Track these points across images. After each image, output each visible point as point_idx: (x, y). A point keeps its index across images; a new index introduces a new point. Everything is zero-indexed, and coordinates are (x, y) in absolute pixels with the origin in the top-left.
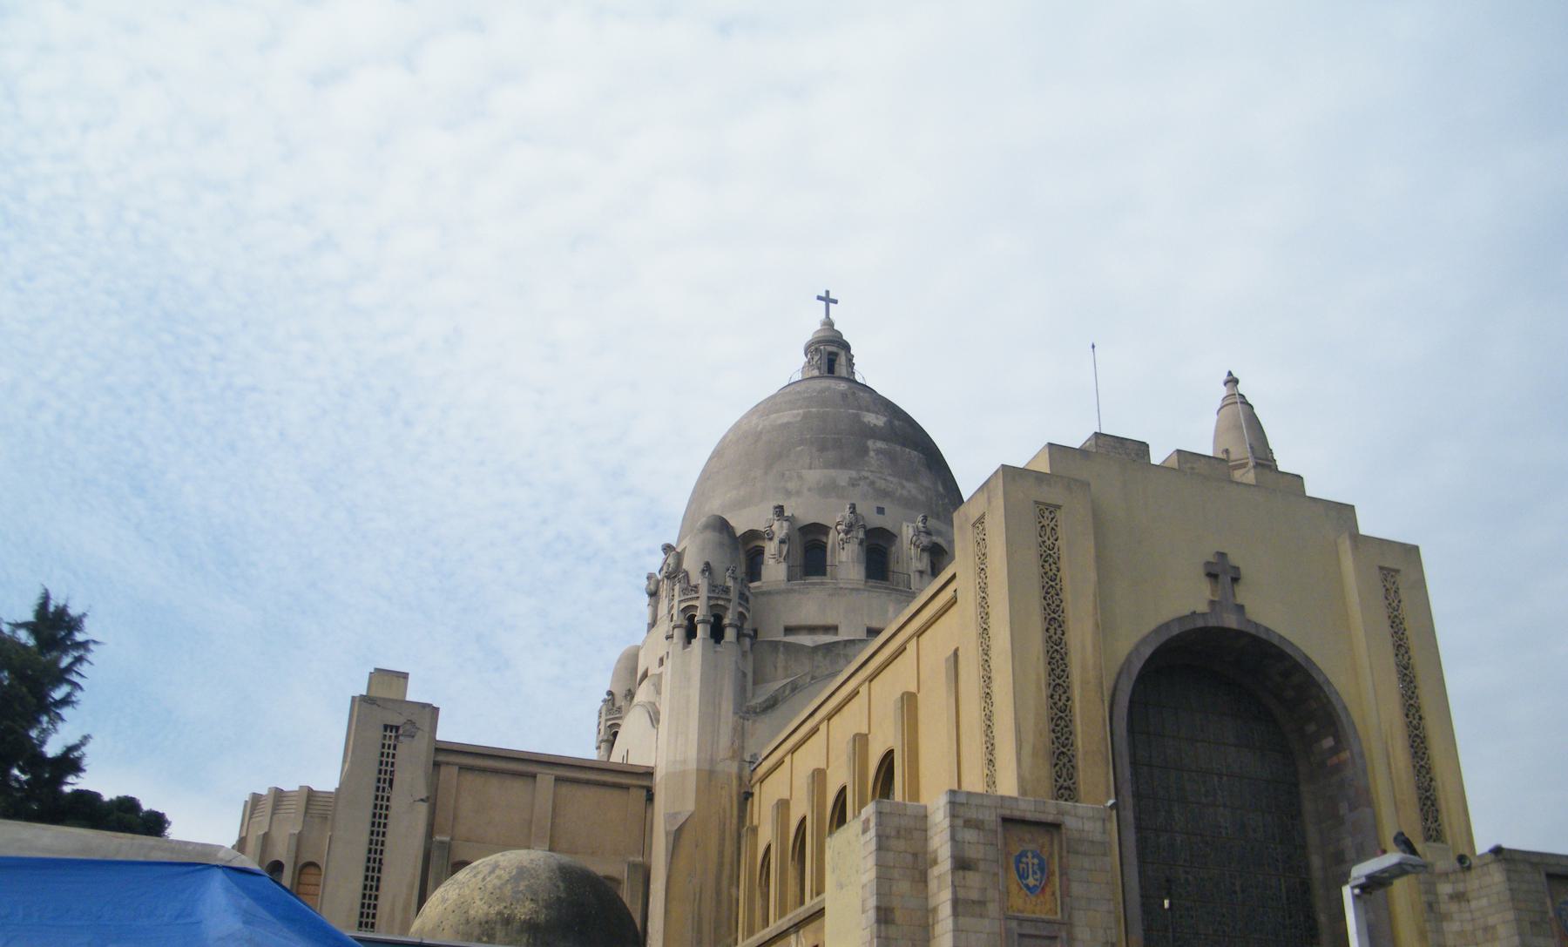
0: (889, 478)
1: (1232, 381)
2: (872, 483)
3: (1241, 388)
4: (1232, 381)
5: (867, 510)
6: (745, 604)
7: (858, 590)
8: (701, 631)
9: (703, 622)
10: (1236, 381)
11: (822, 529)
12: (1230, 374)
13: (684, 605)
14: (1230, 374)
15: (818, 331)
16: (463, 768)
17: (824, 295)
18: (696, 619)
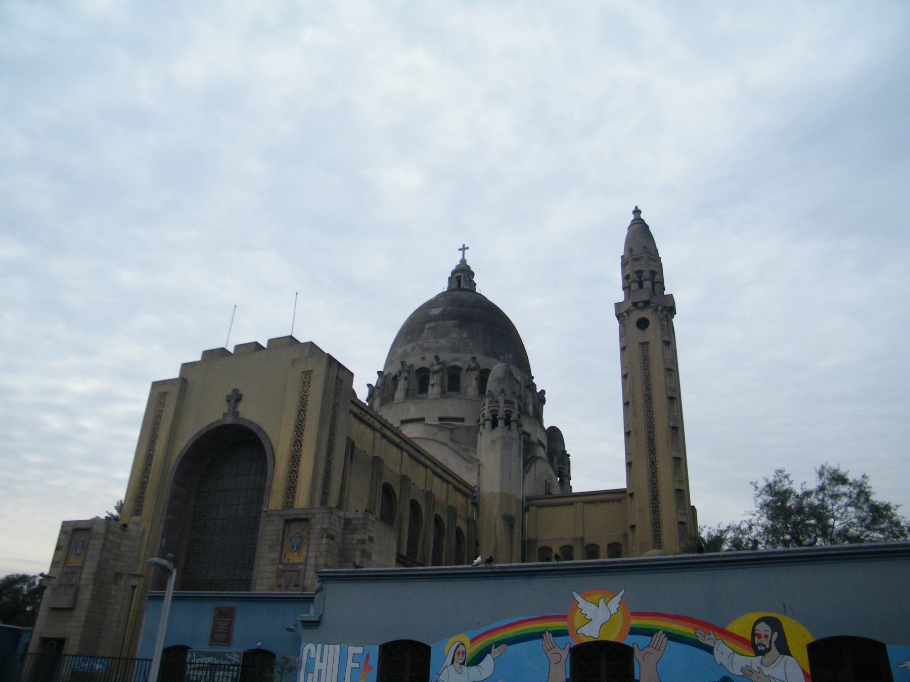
0: (431, 340)
1: (637, 212)
2: (422, 346)
3: (642, 216)
4: (637, 212)
5: (445, 357)
6: (512, 406)
7: (437, 399)
8: (501, 423)
9: (501, 418)
10: (640, 212)
11: (457, 369)
12: (636, 207)
13: (490, 410)
14: (636, 207)
15: (458, 265)
16: (585, 502)
17: (466, 246)
18: (498, 417)
